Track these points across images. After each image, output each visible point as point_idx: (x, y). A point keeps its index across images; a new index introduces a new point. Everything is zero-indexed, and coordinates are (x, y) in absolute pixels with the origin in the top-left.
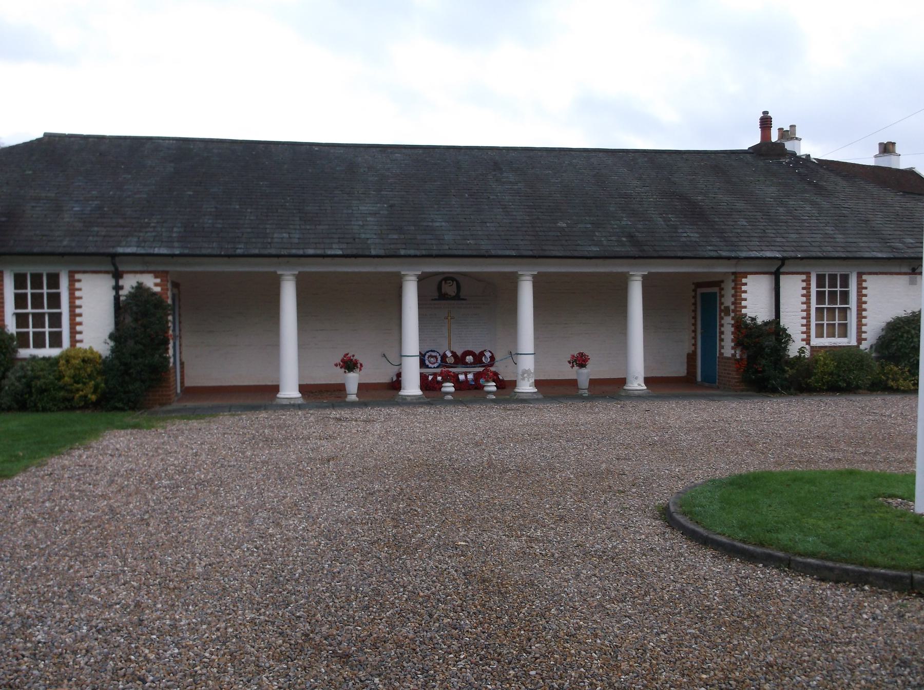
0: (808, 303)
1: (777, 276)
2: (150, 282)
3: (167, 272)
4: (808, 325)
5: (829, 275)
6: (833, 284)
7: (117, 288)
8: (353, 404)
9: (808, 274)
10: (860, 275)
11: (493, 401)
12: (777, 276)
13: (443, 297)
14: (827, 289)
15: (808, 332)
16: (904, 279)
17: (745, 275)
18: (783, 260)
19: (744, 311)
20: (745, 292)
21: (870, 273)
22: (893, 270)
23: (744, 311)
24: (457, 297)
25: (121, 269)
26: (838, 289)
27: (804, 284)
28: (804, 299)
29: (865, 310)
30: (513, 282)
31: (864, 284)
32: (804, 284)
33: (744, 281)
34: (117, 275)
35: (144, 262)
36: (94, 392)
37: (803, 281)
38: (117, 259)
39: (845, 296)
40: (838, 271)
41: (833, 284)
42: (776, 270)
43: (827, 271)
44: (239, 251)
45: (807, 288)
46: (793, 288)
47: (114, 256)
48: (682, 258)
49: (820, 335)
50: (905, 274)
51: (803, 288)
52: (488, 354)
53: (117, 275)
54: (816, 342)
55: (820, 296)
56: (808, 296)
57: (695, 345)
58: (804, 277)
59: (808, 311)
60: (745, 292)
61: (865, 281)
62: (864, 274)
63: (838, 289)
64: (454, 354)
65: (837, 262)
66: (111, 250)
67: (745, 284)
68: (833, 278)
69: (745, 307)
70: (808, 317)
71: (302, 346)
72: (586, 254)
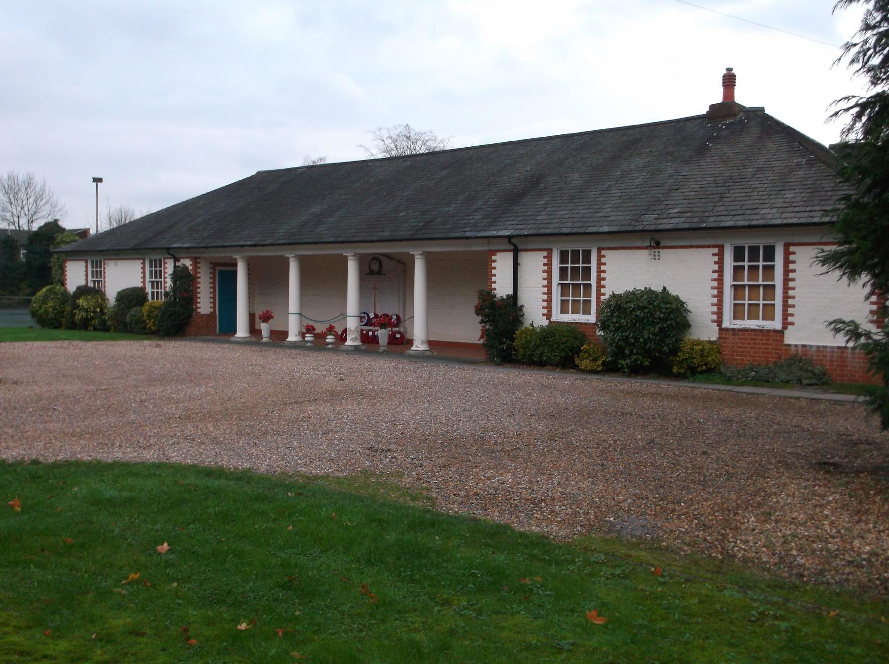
0: (549, 279)
1: (516, 252)
2: (188, 263)
3: (196, 258)
4: (549, 301)
5: (583, 251)
6: (575, 260)
7: (175, 267)
8: (382, 353)
9: (550, 251)
10: (599, 250)
11: (330, 349)
12: (516, 252)
13: (372, 272)
14: (569, 265)
15: (549, 308)
16: (644, 254)
17: (494, 252)
18: (509, 238)
19: (493, 286)
20: (495, 268)
21: (609, 249)
22: (694, 243)
23: (493, 286)
24: (379, 273)
25: (177, 256)
26: (580, 265)
27: (545, 261)
28: (545, 275)
29: (604, 287)
30: (345, 260)
31: (603, 260)
32: (545, 261)
33: (494, 258)
34: (176, 260)
35: (186, 251)
36: (154, 325)
37: (544, 257)
38: (171, 251)
39: (587, 272)
40: (580, 247)
41: (575, 260)
42: (516, 247)
43: (570, 247)
44: (214, 244)
45: (549, 264)
46: (533, 265)
47: (168, 249)
48: (433, 239)
49: (564, 310)
50: (646, 248)
51: (544, 265)
52: (394, 317)
53: (176, 260)
54: (558, 316)
55: (563, 272)
56: (549, 272)
57: (214, 307)
58: (545, 253)
59: (549, 286)
60: (495, 268)
61: (604, 256)
62: (603, 249)
63: (580, 265)
64: (376, 316)
65: (569, 238)
66: (167, 246)
67: (495, 261)
68: (575, 253)
69: (495, 282)
70: (549, 293)
71: (302, 303)
72: (374, 238)
